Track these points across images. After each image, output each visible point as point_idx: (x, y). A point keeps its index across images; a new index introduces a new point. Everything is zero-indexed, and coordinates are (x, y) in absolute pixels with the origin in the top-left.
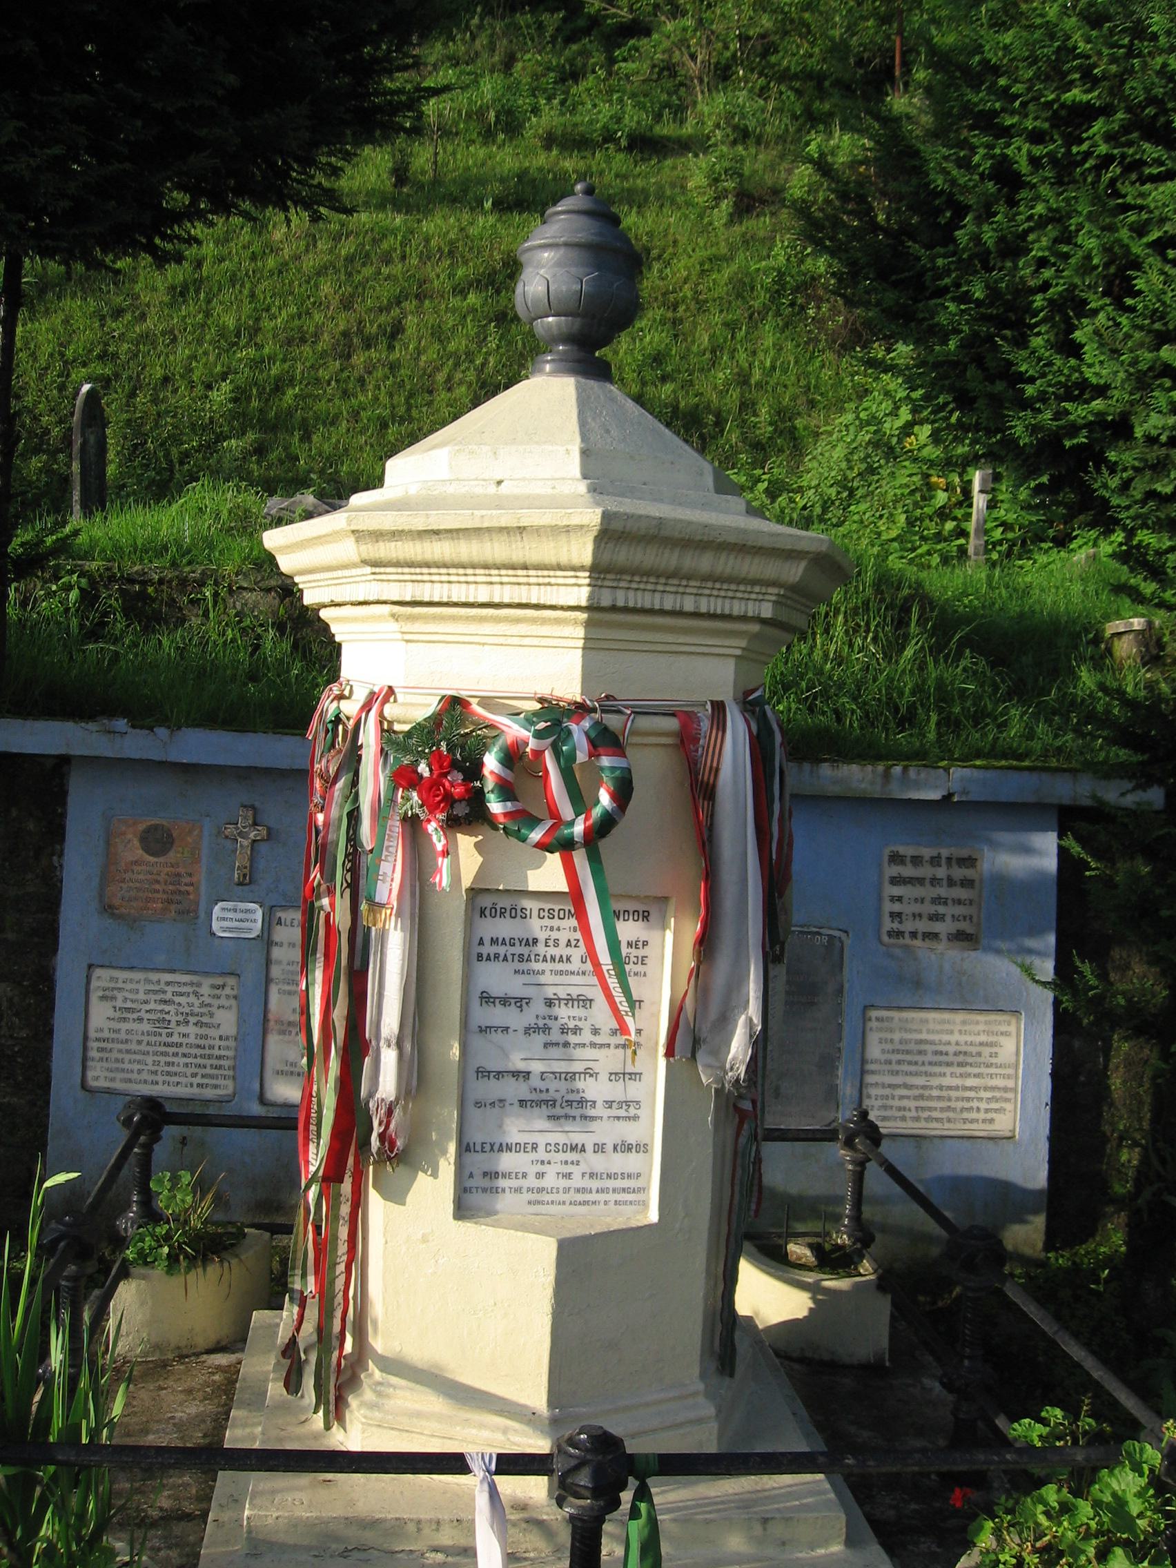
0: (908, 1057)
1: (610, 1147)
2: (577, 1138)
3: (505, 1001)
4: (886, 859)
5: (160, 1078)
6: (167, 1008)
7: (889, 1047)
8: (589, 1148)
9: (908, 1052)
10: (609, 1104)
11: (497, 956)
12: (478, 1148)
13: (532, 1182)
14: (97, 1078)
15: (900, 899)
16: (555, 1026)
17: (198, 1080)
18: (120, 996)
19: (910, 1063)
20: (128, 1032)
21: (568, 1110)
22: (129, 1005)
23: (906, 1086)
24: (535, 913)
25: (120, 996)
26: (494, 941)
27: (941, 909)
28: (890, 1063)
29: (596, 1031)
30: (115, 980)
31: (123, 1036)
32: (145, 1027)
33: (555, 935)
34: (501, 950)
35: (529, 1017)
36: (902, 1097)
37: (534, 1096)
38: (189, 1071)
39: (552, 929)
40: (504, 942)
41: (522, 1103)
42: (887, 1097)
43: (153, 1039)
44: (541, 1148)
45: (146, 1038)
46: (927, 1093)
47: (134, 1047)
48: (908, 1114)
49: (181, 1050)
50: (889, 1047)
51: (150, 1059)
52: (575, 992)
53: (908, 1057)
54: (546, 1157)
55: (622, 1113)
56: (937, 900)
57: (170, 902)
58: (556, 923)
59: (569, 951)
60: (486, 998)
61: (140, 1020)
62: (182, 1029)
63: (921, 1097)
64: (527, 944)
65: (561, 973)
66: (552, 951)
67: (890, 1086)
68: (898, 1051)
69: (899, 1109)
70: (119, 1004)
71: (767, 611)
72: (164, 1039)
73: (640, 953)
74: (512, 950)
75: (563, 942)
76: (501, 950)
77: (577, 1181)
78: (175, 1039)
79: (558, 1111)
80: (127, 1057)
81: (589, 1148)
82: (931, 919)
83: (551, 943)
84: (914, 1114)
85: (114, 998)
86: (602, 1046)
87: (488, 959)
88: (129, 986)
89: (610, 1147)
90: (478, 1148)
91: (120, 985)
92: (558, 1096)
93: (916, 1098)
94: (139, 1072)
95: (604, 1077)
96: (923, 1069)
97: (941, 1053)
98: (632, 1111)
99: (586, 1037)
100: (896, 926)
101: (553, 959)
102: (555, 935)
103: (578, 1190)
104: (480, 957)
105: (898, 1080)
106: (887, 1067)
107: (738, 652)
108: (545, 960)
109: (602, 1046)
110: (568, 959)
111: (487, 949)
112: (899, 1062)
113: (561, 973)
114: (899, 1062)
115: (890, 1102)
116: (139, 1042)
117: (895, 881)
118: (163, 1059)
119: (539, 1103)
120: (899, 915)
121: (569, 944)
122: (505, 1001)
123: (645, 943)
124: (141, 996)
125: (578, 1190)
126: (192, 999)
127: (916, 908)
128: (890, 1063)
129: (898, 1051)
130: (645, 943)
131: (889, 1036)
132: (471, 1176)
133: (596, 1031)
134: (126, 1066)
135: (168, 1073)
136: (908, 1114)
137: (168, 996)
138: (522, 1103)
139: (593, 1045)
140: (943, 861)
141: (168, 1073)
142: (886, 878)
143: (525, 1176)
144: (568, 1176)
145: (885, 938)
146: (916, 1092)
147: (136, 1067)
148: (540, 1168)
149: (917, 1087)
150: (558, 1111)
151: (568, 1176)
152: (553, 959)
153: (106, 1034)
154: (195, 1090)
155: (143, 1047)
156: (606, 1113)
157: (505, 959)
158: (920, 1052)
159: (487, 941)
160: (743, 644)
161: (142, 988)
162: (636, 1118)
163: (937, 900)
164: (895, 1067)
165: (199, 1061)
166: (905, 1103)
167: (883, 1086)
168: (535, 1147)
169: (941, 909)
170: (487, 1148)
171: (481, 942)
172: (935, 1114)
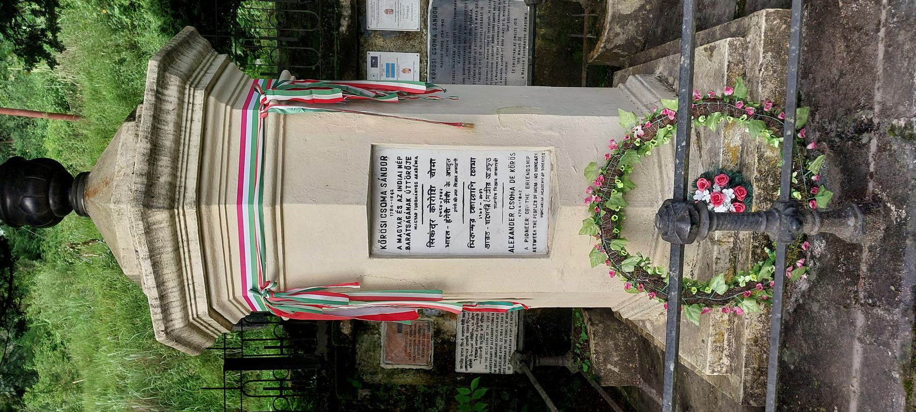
1: (512, 174)
2: (508, 192)
3: (432, 234)
5: (508, 338)
6: (475, 336)
8: (512, 185)
10: (488, 176)
12: (512, 245)
13: (530, 216)
14: (509, 368)
16: (445, 206)
17: (509, 320)
18: (469, 358)
20: (486, 353)
21: (491, 198)
22: (474, 353)
24: (383, 219)
25: (469, 358)
26: (400, 241)
29: (448, 184)
30: (462, 361)
31: (489, 356)
32: (484, 345)
33: (395, 208)
34: (404, 237)
35: (440, 221)
38: (505, 325)
39: (391, 210)
40: (400, 236)
43: (489, 342)
44: (512, 211)
45: (489, 345)
47: (494, 351)
49: (494, 327)
51: (499, 343)
52: (426, 196)
54: (517, 209)
55: (493, 168)
57: (424, 335)
58: (388, 208)
59: (404, 200)
60: (431, 243)
61: (481, 348)
62: (485, 328)
65: (416, 205)
66: (404, 210)
70: (473, 358)
71: (200, 96)
72: (489, 336)
73: (404, 161)
75: (400, 204)
76: (404, 237)
77: (531, 191)
78: (489, 331)
79: (492, 203)
80: (498, 354)
81: (512, 185)
85: (471, 360)
86: (456, 180)
88: (465, 354)
89: (512, 174)
90: (512, 245)
91: (464, 358)
94: (505, 348)
95: (473, 179)
98: (492, 162)
99: (451, 189)
101: (408, 209)
102: (395, 208)
103: (536, 191)
104: (408, 248)
107: (229, 108)
108: (409, 213)
109: (456, 180)
110: (408, 200)
111: (404, 244)
113: (416, 205)
116: (491, 348)
118: (499, 337)
122: (432, 234)
123: (399, 158)
124: (469, 348)
125: (536, 191)
126: (470, 324)
130: (399, 158)
132: (526, 248)
133: (448, 184)
134: (503, 354)
135: (506, 334)
137: (469, 335)
139: (455, 185)
141: (506, 334)
143: (527, 220)
144: (527, 196)
147: (503, 350)
148: (523, 211)
150: (492, 203)
151: (527, 196)
153: (488, 364)
154: (514, 322)
155: (494, 346)
156: (493, 177)
159: (399, 245)
160: (223, 105)
161: (465, 347)
162: (496, 160)
165: (500, 320)
168: (511, 215)
170: (511, 240)
171: (400, 248)
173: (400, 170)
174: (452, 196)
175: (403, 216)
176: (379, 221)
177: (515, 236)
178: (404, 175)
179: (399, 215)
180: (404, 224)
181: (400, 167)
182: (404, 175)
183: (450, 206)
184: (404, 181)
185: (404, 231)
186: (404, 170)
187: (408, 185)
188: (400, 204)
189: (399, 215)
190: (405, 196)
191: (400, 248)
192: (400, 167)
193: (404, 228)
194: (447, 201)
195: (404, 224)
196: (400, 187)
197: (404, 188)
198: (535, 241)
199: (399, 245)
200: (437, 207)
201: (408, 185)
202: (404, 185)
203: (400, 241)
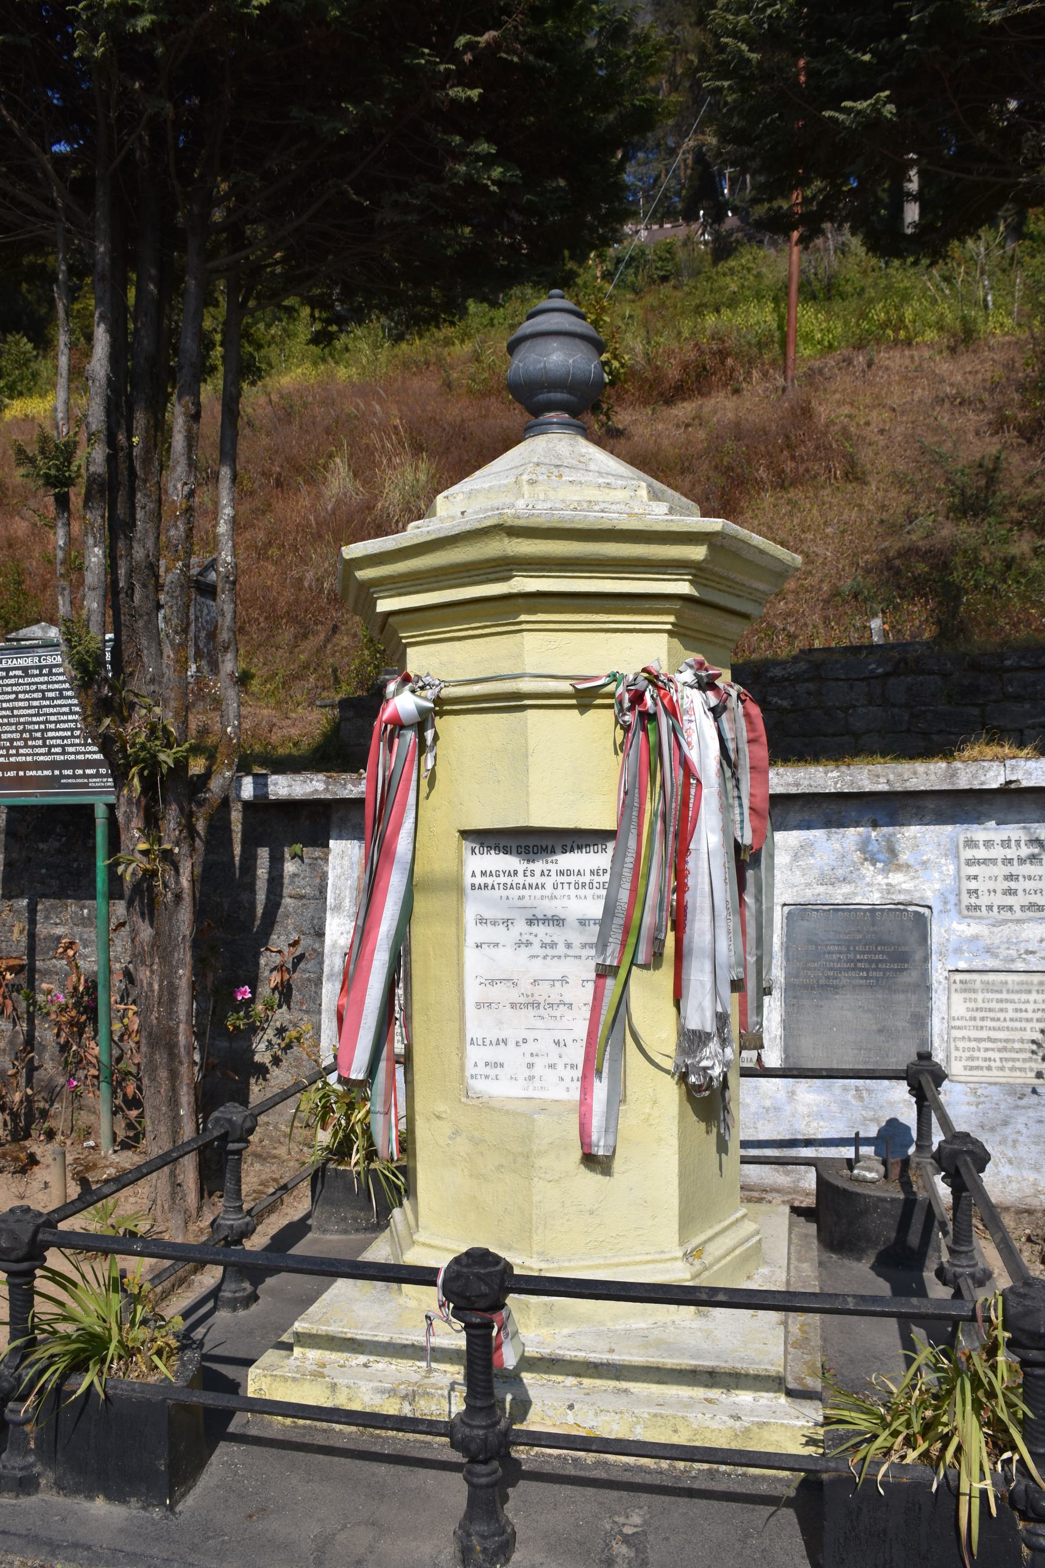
0: (991, 1015)
4: (961, 845)
7: (972, 1005)
9: (990, 1010)
11: (486, 886)
15: (975, 878)
19: (993, 1019)
23: (990, 1040)
26: (483, 874)
27: (1013, 885)
28: (975, 1019)
29: (569, 946)
34: (489, 880)
36: (987, 1050)
37: (522, 1000)
40: (491, 875)
41: (513, 1006)
42: (973, 1049)
46: (1009, 1046)
48: (992, 1064)
50: (972, 1005)
53: (991, 1015)
56: (1010, 877)
59: (543, 879)
63: (1005, 1049)
64: (509, 875)
66: (530, 880)
67: (976, 1040)
68: (981, 1009)
69: (985, 1060)
74: (498, 880)
75: (538, 873)
76: (489, 880)
82: (1004, 894)
83: (528, 873)
84: (998, 1064)
87: (480, 888)
90: (480, 1042)
92: (541, 1000)
93: (999, 1050)
96: (1005, 1024)
97: (1021, 1010)
99: (561, 949)
100: (973, 901)
105: (983, 1034)
106: (973, 1023)
107: (669, 627)
108: (524, 887)
111: (479, 880)
112: (983, 1019)
114: (983, 1019)
115: (976, 1054)
117: (969, 862)
119: (527, 1005)
120: (976, 891)
121: (542, 874)
127: (991, 885)
128: (975, 1019)
129: (981, 1009)
131: (973, 996)
132: (476, 1065)
133: (569, 946)
136: (992, 1064)
138: (513, 1006)
140: (1013, 843)
142: (963, 861)
145: (965, 912)
146: (1000, 1045)
149: (1000, 1040)
152: (531, 886)
157: (493, 887)
158: (1001, 1010)
159: (478, 873)
163: (1010, 877)
164: (981, 1023)
166: (989, 1054)
167: (970, 1039)
169: (1013, 885)
171: (473, 875)
172: (1018, 1064)
173: (588, 872)
174: (549, 952)
175: (520, 879)
176: (513, 844)
177: (489, 1048)
178: (581, 879)
179: (520, 873)
180: (508, 880)
181: (592, 872)
182: (581, 879)
183: (536, 949)
184: (572, 879)
185: (498, 880)
186: (587, 879)
187: (566, 886)
188: (538, 873)
189: (520, 873)
190: (549, 882)
191: (473, 875)
192: (592, 872)
193: (502, 879)
194: (544, 945)
195: (508, 880)
196: (562, 873)
197: (561, 879)
198: (487, 1077)
199: (478, 873)
200: (535, 929)
201: (566, 886)
202: (565, 879)
203: (483, 874)
